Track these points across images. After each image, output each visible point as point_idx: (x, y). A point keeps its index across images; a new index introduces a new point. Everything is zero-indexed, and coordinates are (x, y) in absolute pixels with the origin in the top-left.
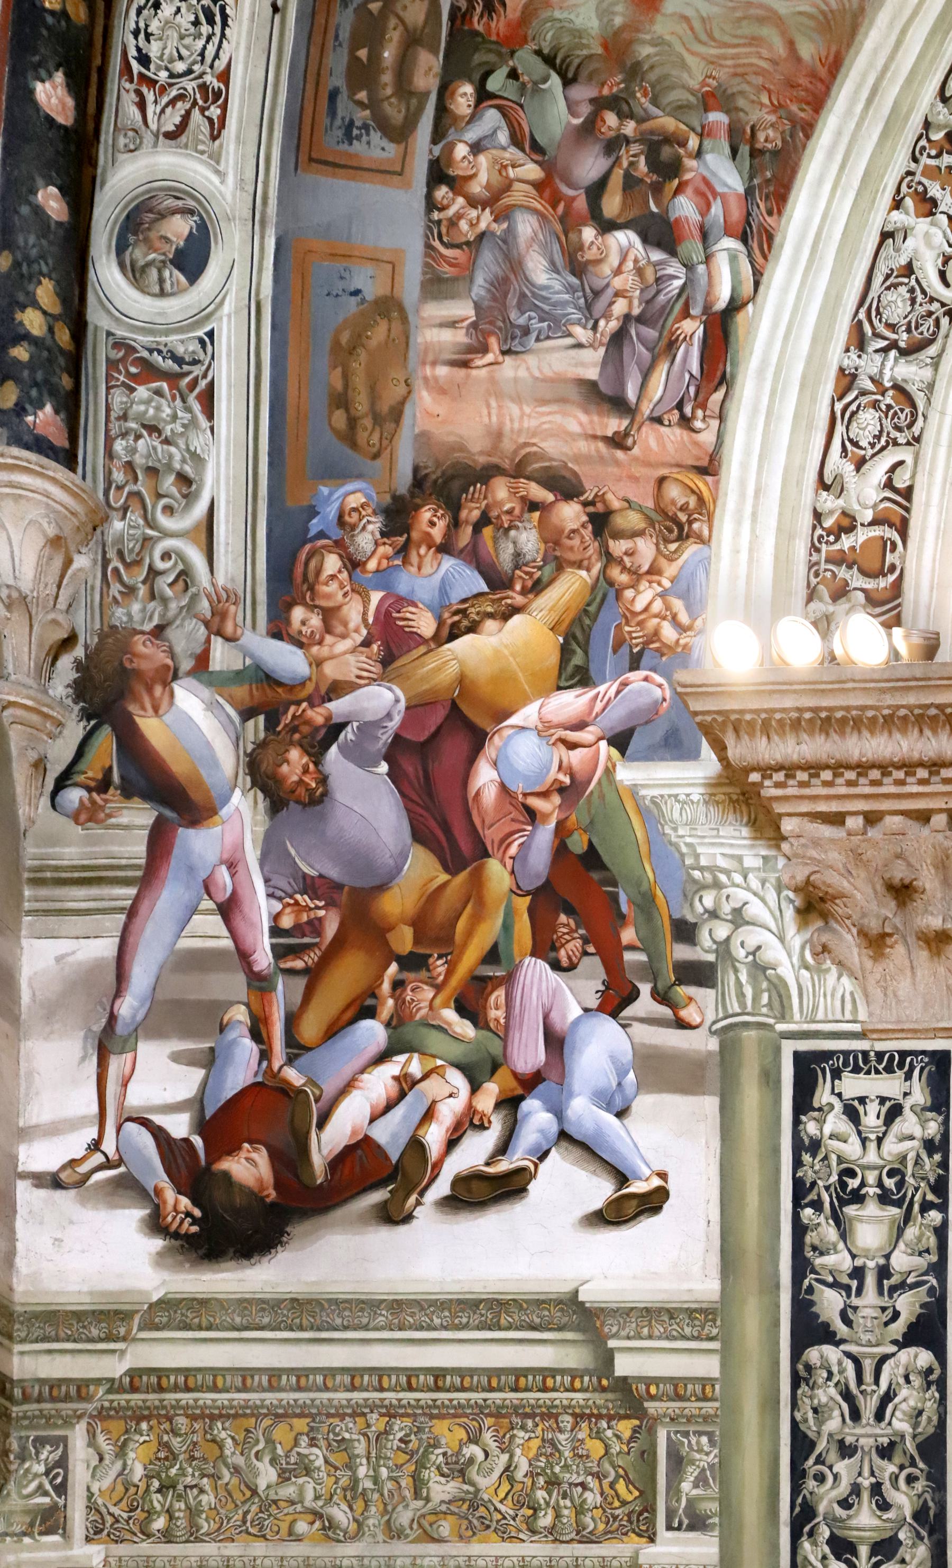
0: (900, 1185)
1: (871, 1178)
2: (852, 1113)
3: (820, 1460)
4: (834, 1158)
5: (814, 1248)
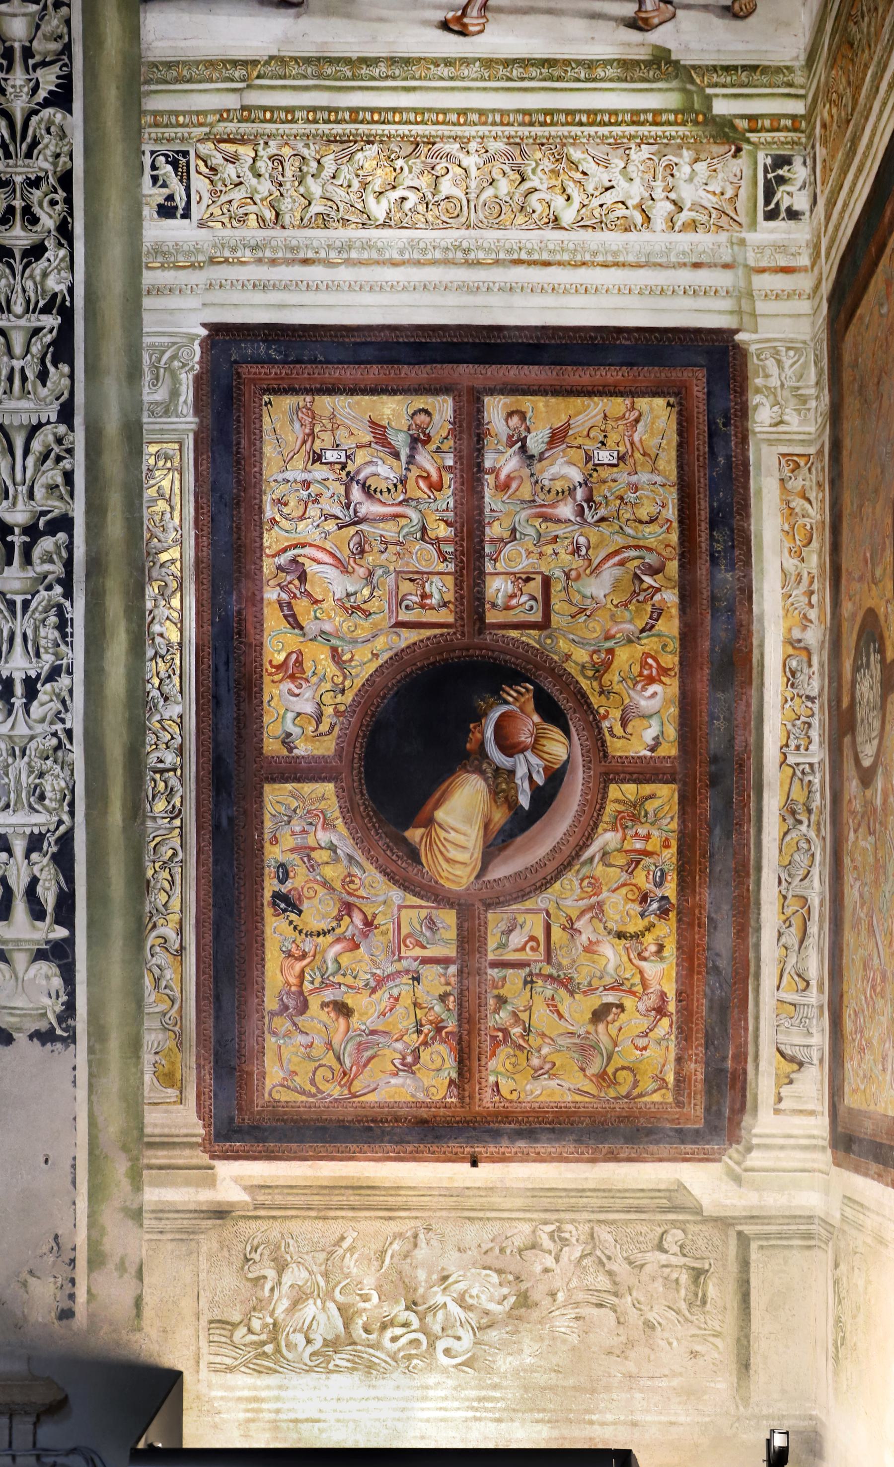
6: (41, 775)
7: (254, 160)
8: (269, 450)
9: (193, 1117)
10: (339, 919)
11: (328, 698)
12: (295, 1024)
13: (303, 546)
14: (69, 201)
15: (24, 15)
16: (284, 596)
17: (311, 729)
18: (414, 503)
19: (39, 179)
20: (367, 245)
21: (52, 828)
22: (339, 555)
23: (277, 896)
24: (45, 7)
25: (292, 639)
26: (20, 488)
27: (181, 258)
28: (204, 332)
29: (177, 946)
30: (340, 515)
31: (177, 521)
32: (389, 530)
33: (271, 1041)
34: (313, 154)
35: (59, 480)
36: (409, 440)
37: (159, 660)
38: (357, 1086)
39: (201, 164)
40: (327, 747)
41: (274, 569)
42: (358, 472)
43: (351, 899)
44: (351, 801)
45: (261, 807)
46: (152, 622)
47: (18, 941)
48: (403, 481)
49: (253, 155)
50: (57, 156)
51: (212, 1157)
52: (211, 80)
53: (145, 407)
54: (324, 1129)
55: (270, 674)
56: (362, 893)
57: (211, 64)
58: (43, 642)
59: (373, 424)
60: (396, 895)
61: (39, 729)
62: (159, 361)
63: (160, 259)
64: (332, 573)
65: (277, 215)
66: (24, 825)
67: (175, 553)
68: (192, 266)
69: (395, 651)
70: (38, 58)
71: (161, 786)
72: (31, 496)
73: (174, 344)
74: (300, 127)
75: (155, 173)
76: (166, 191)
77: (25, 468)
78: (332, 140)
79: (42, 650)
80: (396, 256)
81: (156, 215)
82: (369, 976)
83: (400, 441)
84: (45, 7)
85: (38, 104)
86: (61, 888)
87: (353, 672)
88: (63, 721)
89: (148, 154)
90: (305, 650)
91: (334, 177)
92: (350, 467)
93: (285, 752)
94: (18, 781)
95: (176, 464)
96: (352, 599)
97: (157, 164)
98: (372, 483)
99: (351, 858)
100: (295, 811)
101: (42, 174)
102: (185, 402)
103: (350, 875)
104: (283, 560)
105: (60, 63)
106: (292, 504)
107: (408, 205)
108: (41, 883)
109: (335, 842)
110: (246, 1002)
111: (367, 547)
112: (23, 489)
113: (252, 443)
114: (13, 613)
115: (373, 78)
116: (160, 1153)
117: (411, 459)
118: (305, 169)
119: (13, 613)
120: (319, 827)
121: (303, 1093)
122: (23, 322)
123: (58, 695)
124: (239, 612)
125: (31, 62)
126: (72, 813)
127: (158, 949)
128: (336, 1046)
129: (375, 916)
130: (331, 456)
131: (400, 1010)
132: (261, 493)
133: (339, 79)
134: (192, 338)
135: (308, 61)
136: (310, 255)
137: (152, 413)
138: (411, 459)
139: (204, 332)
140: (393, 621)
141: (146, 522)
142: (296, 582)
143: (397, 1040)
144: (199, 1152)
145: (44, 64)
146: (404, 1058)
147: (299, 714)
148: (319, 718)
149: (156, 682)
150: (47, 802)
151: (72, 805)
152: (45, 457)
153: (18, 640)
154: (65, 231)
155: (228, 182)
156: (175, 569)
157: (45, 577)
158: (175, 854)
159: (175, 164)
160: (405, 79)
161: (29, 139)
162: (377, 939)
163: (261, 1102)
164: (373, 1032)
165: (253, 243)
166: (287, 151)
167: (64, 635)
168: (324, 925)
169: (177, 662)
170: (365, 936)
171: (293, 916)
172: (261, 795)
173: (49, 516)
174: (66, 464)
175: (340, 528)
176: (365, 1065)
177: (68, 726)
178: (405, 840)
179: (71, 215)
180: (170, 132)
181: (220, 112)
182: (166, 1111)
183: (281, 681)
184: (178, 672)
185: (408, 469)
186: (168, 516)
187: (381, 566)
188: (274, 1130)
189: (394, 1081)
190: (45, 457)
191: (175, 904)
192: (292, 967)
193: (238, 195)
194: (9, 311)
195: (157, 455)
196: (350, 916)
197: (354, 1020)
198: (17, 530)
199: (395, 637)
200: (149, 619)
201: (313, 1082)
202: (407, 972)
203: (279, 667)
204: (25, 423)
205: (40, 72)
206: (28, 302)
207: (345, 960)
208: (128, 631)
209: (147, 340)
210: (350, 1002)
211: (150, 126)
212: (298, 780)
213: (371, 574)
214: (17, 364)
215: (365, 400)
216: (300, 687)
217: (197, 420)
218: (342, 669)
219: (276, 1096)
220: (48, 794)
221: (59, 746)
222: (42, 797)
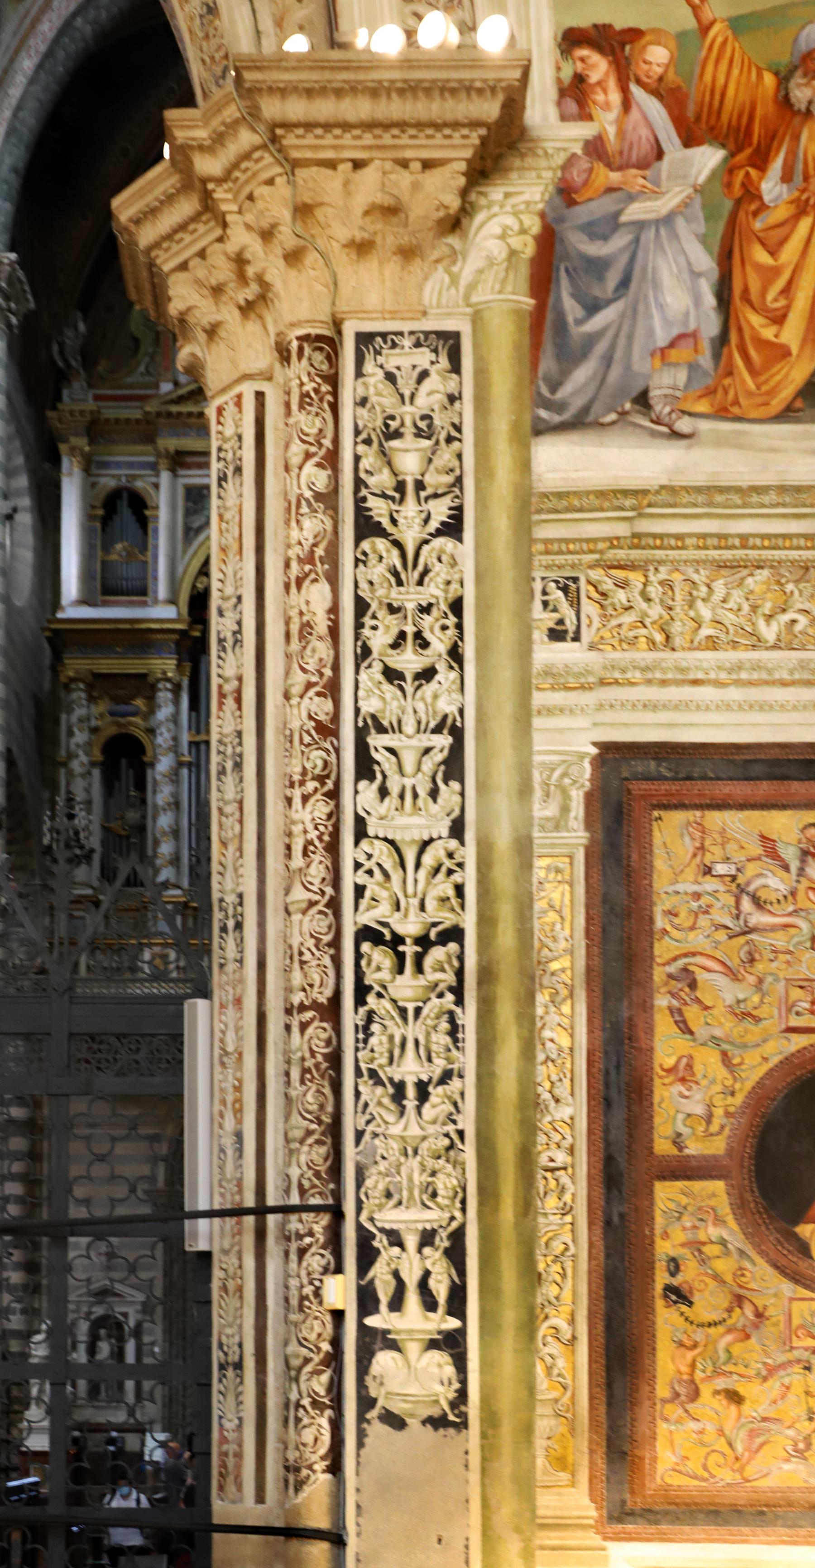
0: (430, 426)
1: (408, 422)
2: (390, 377)
3: (374, 617)
4: (377, 408)
5: (367, 472)
6: (433, 1174)
7: (645, 585)
8: (660, 863)
9: (586, 1501)
10: (730, 1310)
11: (718, 1101)
12: (686, 1411)
13: (694, 954)
14: (459, 626)
15: (417, 450)
16: (675, 1003)
17: (702, 1129)
18: (802, 914)
19: (430, 605)
20: (756, 666)
21: (444, 1224)
22: (729, 963)
23: (670, 1289)
24: (437, 443)
25: (683, 1044)
26: (411, 901)
27: (571, 680)
28: (594, 751)
29: (569, 1336)
30: (730, 925)
31: (567, 932)
32: (780, 940)
33: (662, 1428)
34: (704, 579)
35: (451, 892)
36: (799, 853)
37: (550, 1064)
38: (749, 1472)
39: (591, 588)
40: (718, 1147)
41: (665, 978)
42: (748, 884)
43: (741, 1292)
44: (741, 1198)
45: (652, 1204)
46: (542, 1028)
47: (410, 1331)
48: (793, 893)
49: (643, 579)
50: (448, 583)
51: (605, 1539)
52: (602, 509)
53: (536, 822)
54: (716, 1513)
55: (661, 1077)
56: (753, 1286)
57: (601, 494)
58: (434, 1047)
59: (763, 838)
60: (787, 1288)
61: (431, 1129)
62: (549, 777)
63: (550, 681)
64: (722, 981)
65: (668, 638)
66: (416, 1221)
67: (565, 962)
68: (582, 687)
69: (785, 1054)
70: (429, 491)
71: (552, 1184)
72: (422, 907)
73: (564, 761)
74: (691, 554)
75: (545, 598)
76: (556, 616)
77: (416, 881)
78: (723, 565)
79: (433, 1055)
80: (786, 676)
81: (546, 639)
82: (760, 1366)
83: (790, 854)
84: (437, 443)
85: (431, 534)
86: (453, 1281)
87: (743, 1075)
88: (454, 1122)
89: (538, 580)
90: (695, 1054)
91: (724, 601)
92: (741, 880)
93: (675, 1152)
94: (410, 1180)
95: (567, 877)
96: (742, 1005)
97: (548, 590)
98: (763, 895)
99: (742, 1252)
100: (685, 1208)
101: (433, 601)
102: (576, 818)
103: (741, 1269)
104: (672, 969)
105: (451, 495)
106: (683, 915)
107: (798, 628)
108: (433, 1276)
109: (726, 1237)
110: (637, 1391)
111: (757, 956)
112: (415, 902)
113: (642, 857)
114: (405, 1018)
115: (763, 506)
116: (553, 1534)
117: (801, 872)
118: (695, 593)
119: (405, 1018)
120: (710, 1223)
121: (695, 1477)
122: (414, 742)
123: (449, 1098)
124: (630, 1019)
125: (423, 494)
126: (464, 1210)
127: (550, 1339)
128: (727, 1432)
129: (765, 1307)
130: (721, 869)
131: (791, 1398)
132: (652, 904)
133: (729, 507)
134: (582, 756)
135: (699, 490)
136: (700, 675)
137: (543, 828)
138: (801, 872)
139: (594, 751)
140: (783, 1027)
141: (536, 932)
142: (687, 990)
143: (789, 1427)
144: (591, 1533)
145: (436, 496)
146: (795, 1445)
147: (689, 1115)
148: (709, 1118)
149: (547, 1085)
150: (439, 1199)
151: (463, 1202)
152: (437, 870)
153: (410, 1045)
154: (455, 655)
155: (618, 607)
156: (566, 977)
157: (436, 985)
158: (567, 1249)
159: (565, 589)
160: (796, 506)
161: (420, 568)
162: (768, 1329)
163: (653, 1486)
164: (765, 1419)
165: (643, 664)
166: (677, 577)
167: (455, 1040)
168: (714, 1317)
169: (568, 1065)
170: (756, 1326)
171: (684, 1308)
172: (651, 1193)
173: (440, 928)
174: (457, 878)
175: (730, 937)
176: (757, 1451)
177: (460, 1126)
178: (796, 1236)
179: (462, 639)
180: (560, 559)
181: (610, 539)
182: (560, 1494)
183: (671, 1084)
184: (569, 1075)
185: (798, 881)
186: (558, 926)
187: (771, 974)
188: (666, 1513)
189: (787, 1467)
190: (437, 870)
191: (567, 1295)
192: (684, 1357)
193: (628, 618)
194: (400, 731)
195: (548, 869)
196: (740, 1307)
197: (746, 1408)
198: (408, 941)
199: (785, 1042)
200: (539, 1024)
201: (705, 1468)
202: (799, 1361)
203: (669, 1071)
204: (417, 838)
205: (432, 505)
206: (419, 723)
207: (736, 1350)
208: (519, 1037)
209: (537, 759)
210: (742, 1391)
211: (541, 553)
212: (688, 1178)
213: (761, 981)
214: (408, 782)
215: (756, 814)
216: (689, 1089)
217: (587, 835)
218: (732, 1072)
219: (669, 1481)
220: (441, 1192)
221: (451, 1147)
222: (434, 1195)
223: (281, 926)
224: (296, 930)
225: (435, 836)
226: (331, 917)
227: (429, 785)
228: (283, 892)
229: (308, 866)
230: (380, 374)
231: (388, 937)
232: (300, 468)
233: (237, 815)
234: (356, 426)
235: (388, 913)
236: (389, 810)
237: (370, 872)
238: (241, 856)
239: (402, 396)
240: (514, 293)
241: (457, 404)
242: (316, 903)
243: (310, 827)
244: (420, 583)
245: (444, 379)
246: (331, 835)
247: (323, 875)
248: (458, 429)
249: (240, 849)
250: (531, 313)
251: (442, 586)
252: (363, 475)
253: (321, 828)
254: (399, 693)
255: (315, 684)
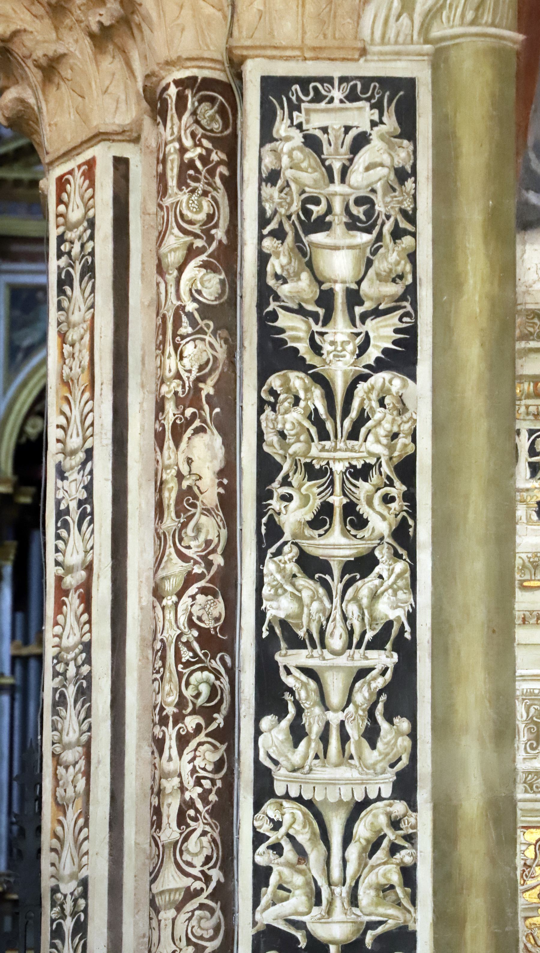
0: (369, 213)
1: (338, 207)
3: (286, 482)
4: (293, 186)
5: (277, 277)
15: (350, 247)
19: (367, 467)
24: (380, 237)
26: (337, 890)
35: (395, 878)
50: (395, 436)
53: (521, 777)
70: (368, 305)
72: (354, 900)
77: (344, 862)
84: (380, 237)
89: (524, 434)
101: (372, 461)
105: (400, 312)
112: (342, 892)
122: (342, 661)
125: (358, 310)
141: (522, 938)
145: (376, 313)
152: (375, 846)
161: (354, 414)
173: (380, 930)
179: (414, 516)
190: (375, 846)
194: (323, 646)
204: (346, 798)
205: (371, 325)
206: (351, 633)
209: (522, 686)
223: (144, 927)
224: (166, 934)
225: (373, 795)
226: (218, 913)
227: (364, 723)
228: (148, 879)
229: (186, 839)
230: (298, 138)
231: (303, 944)
232: (181, 269)
233: (82, 763)
234: (262, 211)
235: (302, 908)
236: (306, 757)
237: (277, 848)
238: (86, 824)
239: (329, 170)
240: (493, 25)
241: (409, 184)
242: (198, 893)
243: (189, 782)
244: (354, 435)
245: (391, 147)
246: (219, 792)
247: (207, 852)
248: (411, 218)
249: (85, 814)
250: (518, 54)
251: (384, 441)
252: (271, 282)
253: (207, 784)
254: (321, 591)
255: (200, 577)
